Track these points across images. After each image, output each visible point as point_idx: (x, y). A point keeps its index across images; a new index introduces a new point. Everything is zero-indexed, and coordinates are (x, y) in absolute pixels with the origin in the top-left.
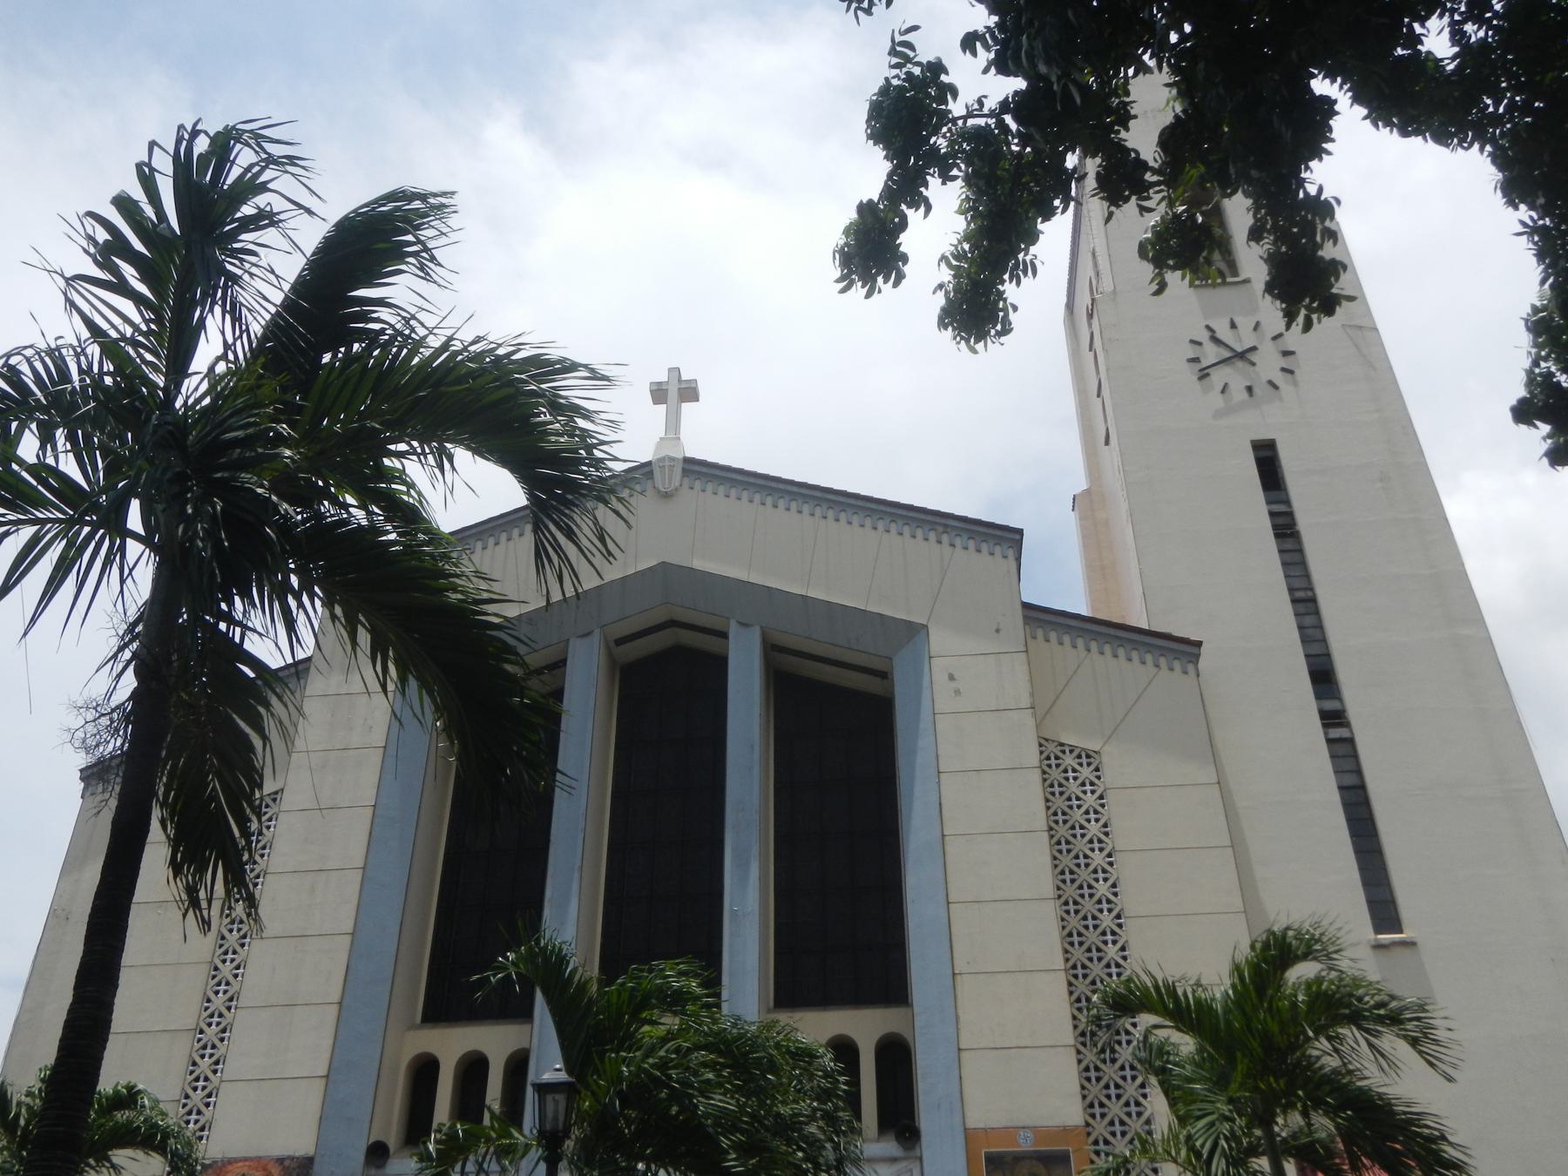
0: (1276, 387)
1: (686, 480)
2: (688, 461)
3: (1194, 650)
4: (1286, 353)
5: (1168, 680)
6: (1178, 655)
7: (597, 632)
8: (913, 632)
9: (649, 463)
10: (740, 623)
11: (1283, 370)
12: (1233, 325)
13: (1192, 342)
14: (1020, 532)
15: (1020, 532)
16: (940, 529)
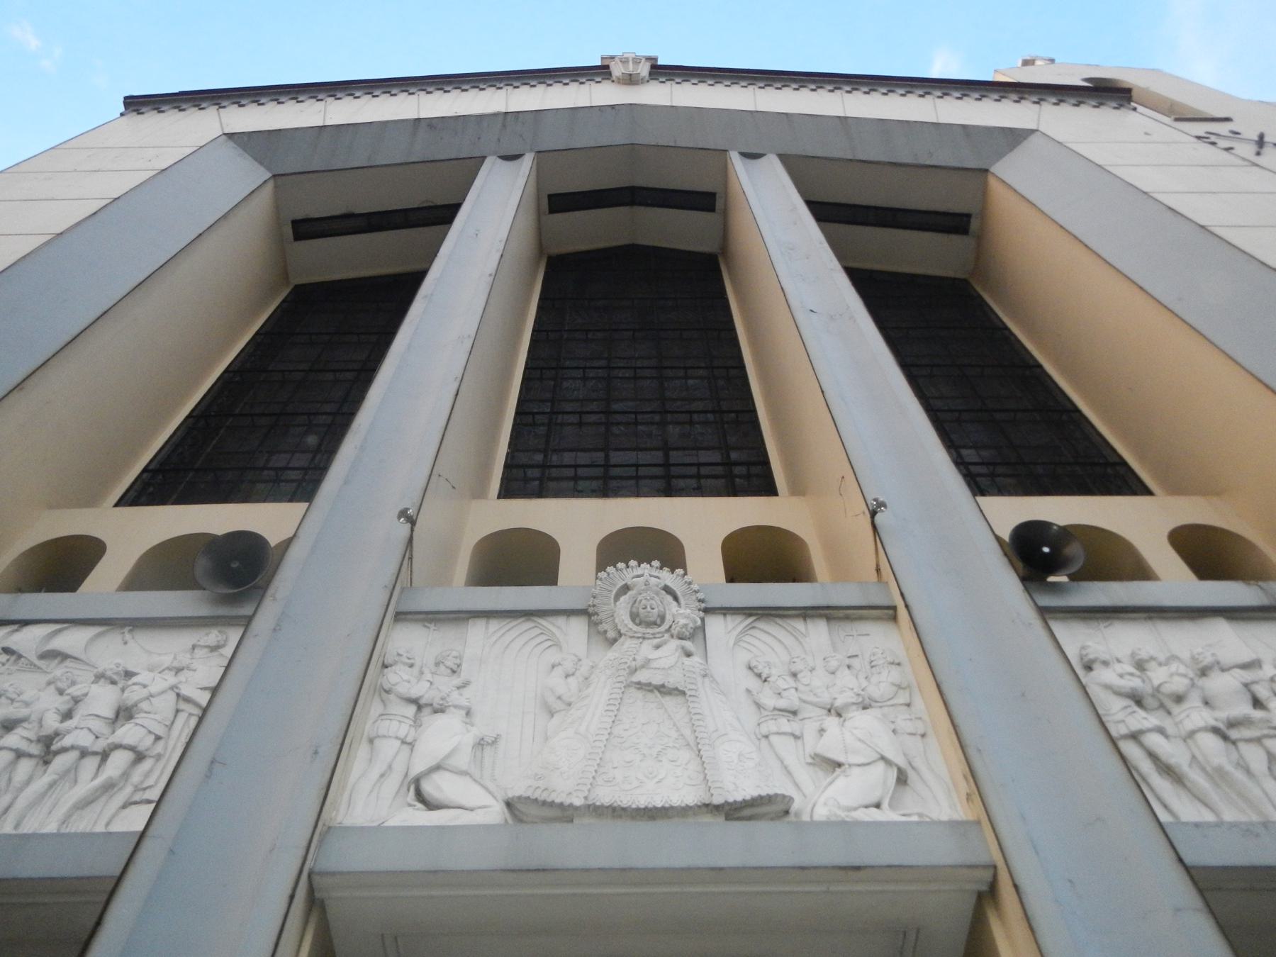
7: (528, 161)
8: (1014, 137)
10: (746, 155)
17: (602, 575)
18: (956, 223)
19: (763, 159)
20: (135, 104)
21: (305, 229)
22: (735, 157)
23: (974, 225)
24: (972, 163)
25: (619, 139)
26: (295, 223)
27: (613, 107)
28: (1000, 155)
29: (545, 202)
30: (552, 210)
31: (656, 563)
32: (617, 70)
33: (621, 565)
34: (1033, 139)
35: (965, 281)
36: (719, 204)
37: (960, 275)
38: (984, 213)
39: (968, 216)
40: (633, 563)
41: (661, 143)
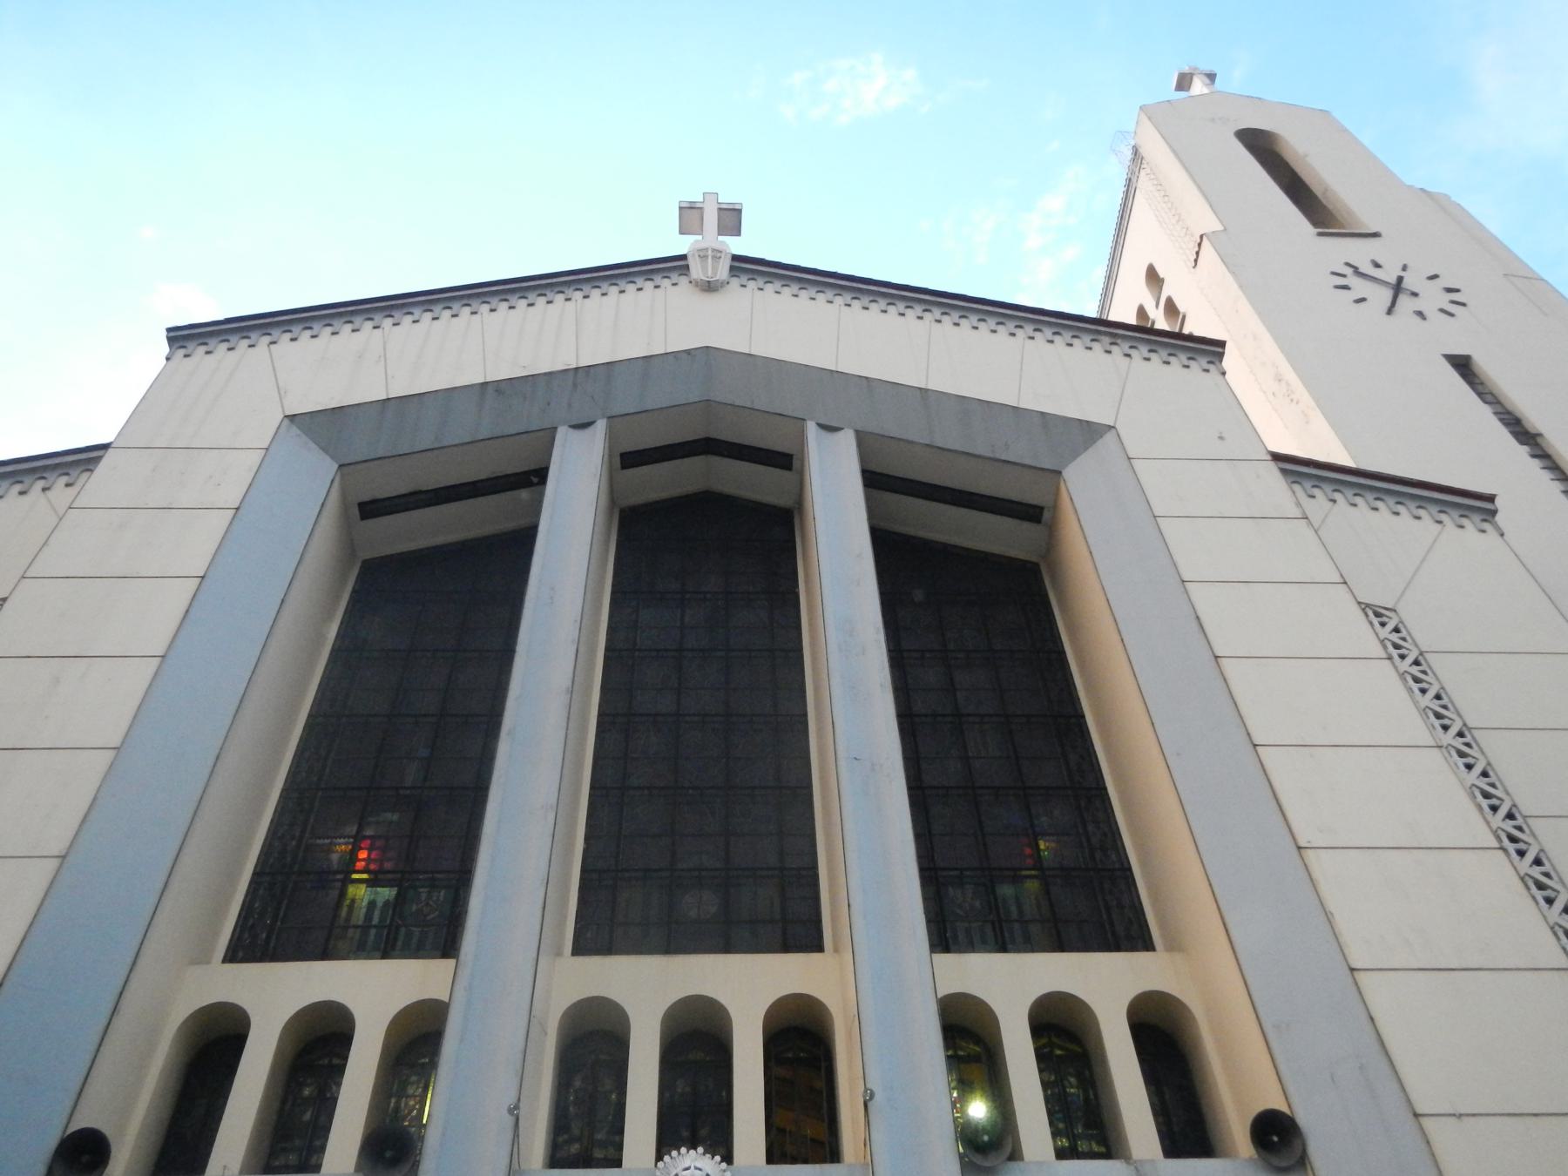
0: (1452, 315)
1: (735, 282)
2: (736, 258)
3: (1488, 506)
4: (1449, 290)
5: (1460, 539)
6: (1466, 511)
7: (601, 426)
8: (1090, 433)
9: (683, 257)
11: (1453, 302)
12: (1377, 265)
13: (1334, 273)
14: (1222, 344)
15: (1222, 344)
16: (1107, 340)
17: (660, 1164)
18: (1032, 513)
19: (840, 434)
20: (182, 338)
21: (371, 509)
22: (811, 429)
23: (1046, 515)
24: (1047, 464)
25: (694, 396)
26: (362, 505)
27: (688, 352)
28: (1075, 455)
29: (618, 459)
30: (624, 466)
31: (701, 1150)
32: (696, 272)
33: (674, 1153)
34: (1109, 437)
35: (1037, 565)
36: (796, 464)
37: (1034, 559)
38: (1055, 507)
39: (1042, 509)
40: (683, 1150)
41: (737, 403)
